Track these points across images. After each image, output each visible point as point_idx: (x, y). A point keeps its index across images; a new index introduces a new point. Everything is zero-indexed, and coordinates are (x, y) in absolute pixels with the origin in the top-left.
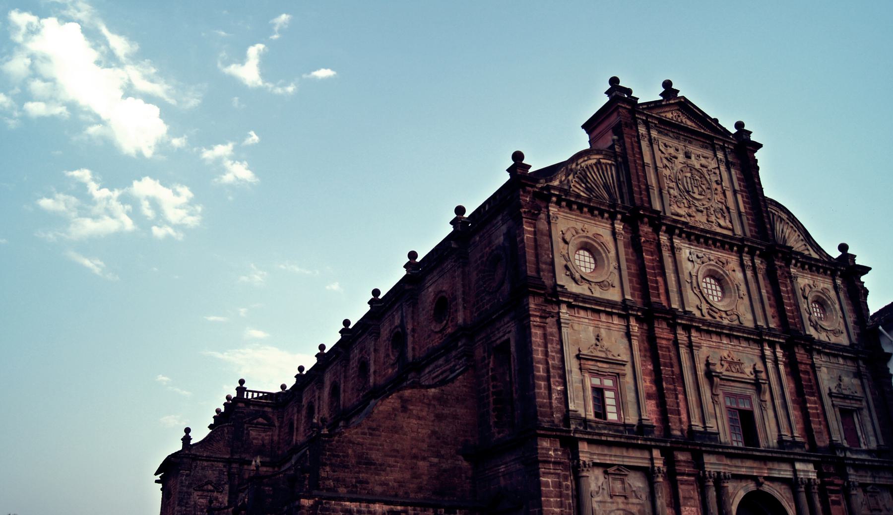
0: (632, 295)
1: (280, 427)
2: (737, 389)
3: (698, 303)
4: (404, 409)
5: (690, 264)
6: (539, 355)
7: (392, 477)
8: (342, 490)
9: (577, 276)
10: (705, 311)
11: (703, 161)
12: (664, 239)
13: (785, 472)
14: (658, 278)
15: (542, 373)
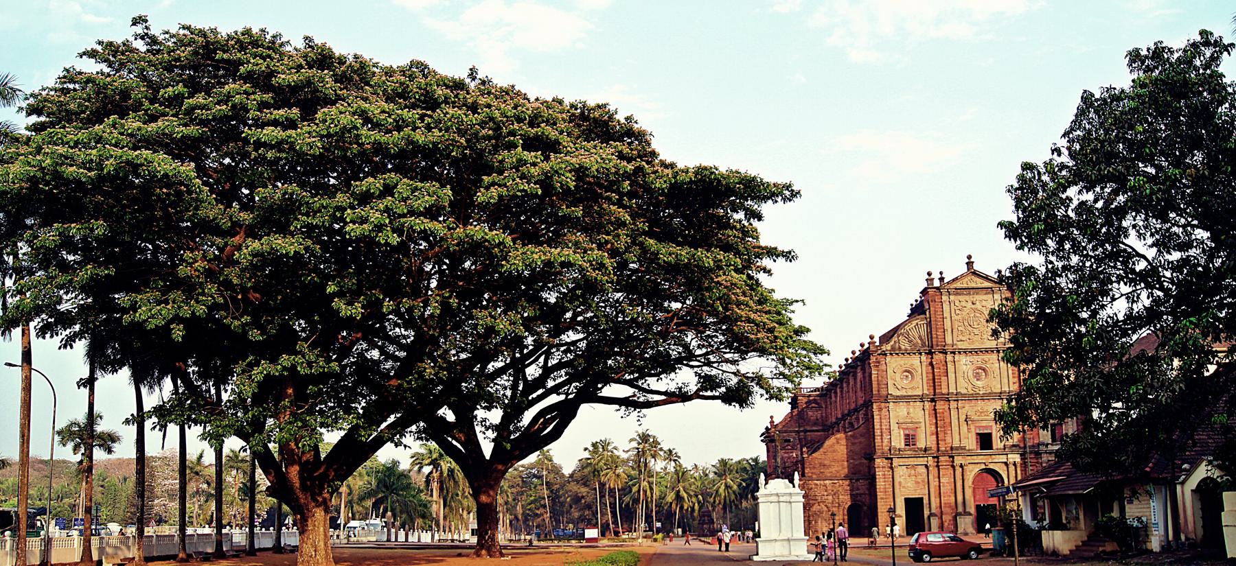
0: (928, 390)
1: (826, 408)
2: (984, 424)
3: (966, 385)
4: (838, 443)
5: (965, 367)
6: (877, 426)
7: (833, 470)
8: (814, 476)
9: (899, 387)
10: (969, 390)
11: (984, 303)
12: (949, 357)
13: (1003, 458)
14: (943, 378)
15: (879, 434)
